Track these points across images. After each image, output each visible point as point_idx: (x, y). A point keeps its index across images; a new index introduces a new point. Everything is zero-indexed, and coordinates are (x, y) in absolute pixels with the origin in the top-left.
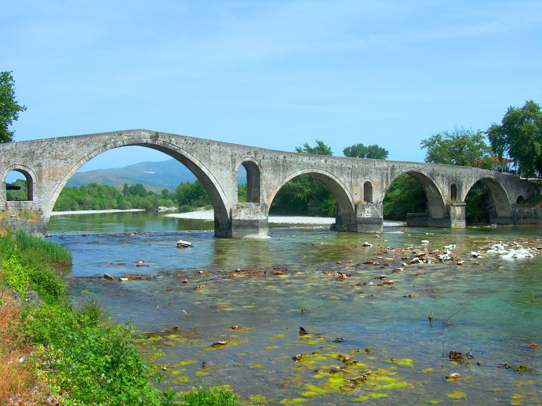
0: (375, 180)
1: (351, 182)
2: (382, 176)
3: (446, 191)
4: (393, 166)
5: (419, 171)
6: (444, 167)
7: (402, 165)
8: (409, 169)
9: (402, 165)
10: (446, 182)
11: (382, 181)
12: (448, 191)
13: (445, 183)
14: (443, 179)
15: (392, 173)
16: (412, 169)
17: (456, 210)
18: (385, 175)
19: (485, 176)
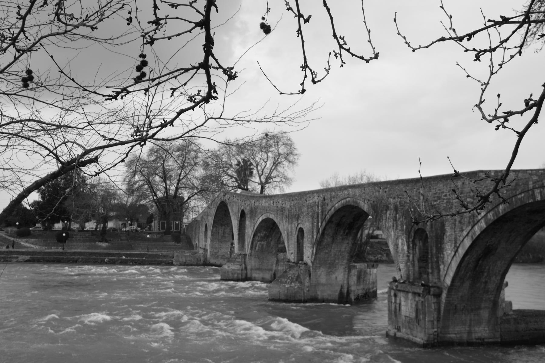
0: (306, 226)
1: (288, 230)
2: (313, 217)
3: (403, 250)
4: (324, 198)
5: (356, 202)
6: (397, 187)
7: (333, 194)
8: (343, 201)
9: (333, 194)
10: (402, 225)
11: (313, 227)
12: (405, 248)
13: (399, 227)
14: (396, 217)
15: (322, 212)
16: (348, 199)
17: (400, 304)
18: (316, 215)
19: (533, 195)
